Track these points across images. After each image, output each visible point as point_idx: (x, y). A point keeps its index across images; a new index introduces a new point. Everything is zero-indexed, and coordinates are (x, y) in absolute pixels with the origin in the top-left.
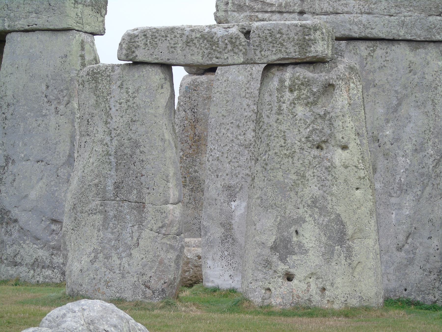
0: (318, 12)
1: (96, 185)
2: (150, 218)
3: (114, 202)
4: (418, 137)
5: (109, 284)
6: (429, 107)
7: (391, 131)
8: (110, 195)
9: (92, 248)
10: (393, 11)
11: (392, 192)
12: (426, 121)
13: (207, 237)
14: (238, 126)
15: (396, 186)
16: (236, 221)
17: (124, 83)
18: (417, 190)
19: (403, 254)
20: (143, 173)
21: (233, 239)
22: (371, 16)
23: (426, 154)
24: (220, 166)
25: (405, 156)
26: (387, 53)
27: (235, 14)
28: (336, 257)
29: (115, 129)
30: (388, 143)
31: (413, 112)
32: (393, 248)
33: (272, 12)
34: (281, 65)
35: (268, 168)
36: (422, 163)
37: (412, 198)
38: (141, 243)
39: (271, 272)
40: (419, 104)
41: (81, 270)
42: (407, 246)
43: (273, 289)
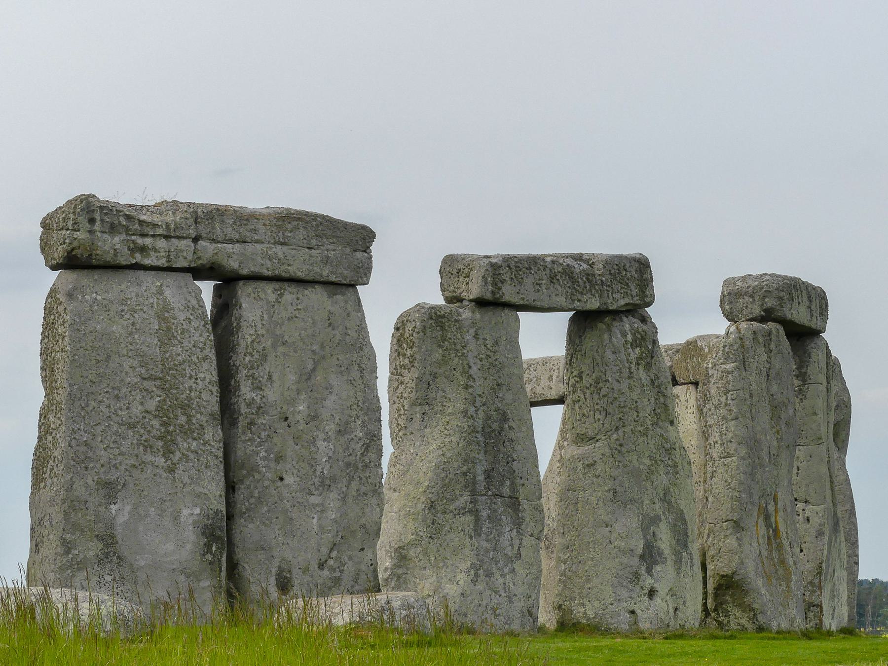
0: (220, 239)
1: (465, 474)
2: (527, 519)
3: (484, 498)
4: (343, 413)
5: (498, 612)
6: (355, 374)
7: (305, 405)
8: (481, 487)
9: (469, 563)
10: (314, 242)
11: (312, 488)
12: (352, 393)
13: (70, 556)
14: (117, 397)
15: (317, 481)
16: (119, 531)
17: (480, 332)
18: (342, 485)
19: (326, 573)
20: (515, 457)
21: (118, 557)
22: (286, 247)
23: (352, 436)
24: (90, 454)
25: (327, 439)
26: (298, 299)
27: (106, 236)
28: (684, 566)
29: (480, 396)
30: (302, 421)
31: (335, 381)
32: (314, 565)
33: (153, 236)
34: (616, 314)
35: (624, 450)
36: (348, 448)
37: (336, 496)
38: (523, 554)
39: (638, 589)
40: (343, 369)
41: (462, 594)
42: (331, 562)
43: (638, 612)
